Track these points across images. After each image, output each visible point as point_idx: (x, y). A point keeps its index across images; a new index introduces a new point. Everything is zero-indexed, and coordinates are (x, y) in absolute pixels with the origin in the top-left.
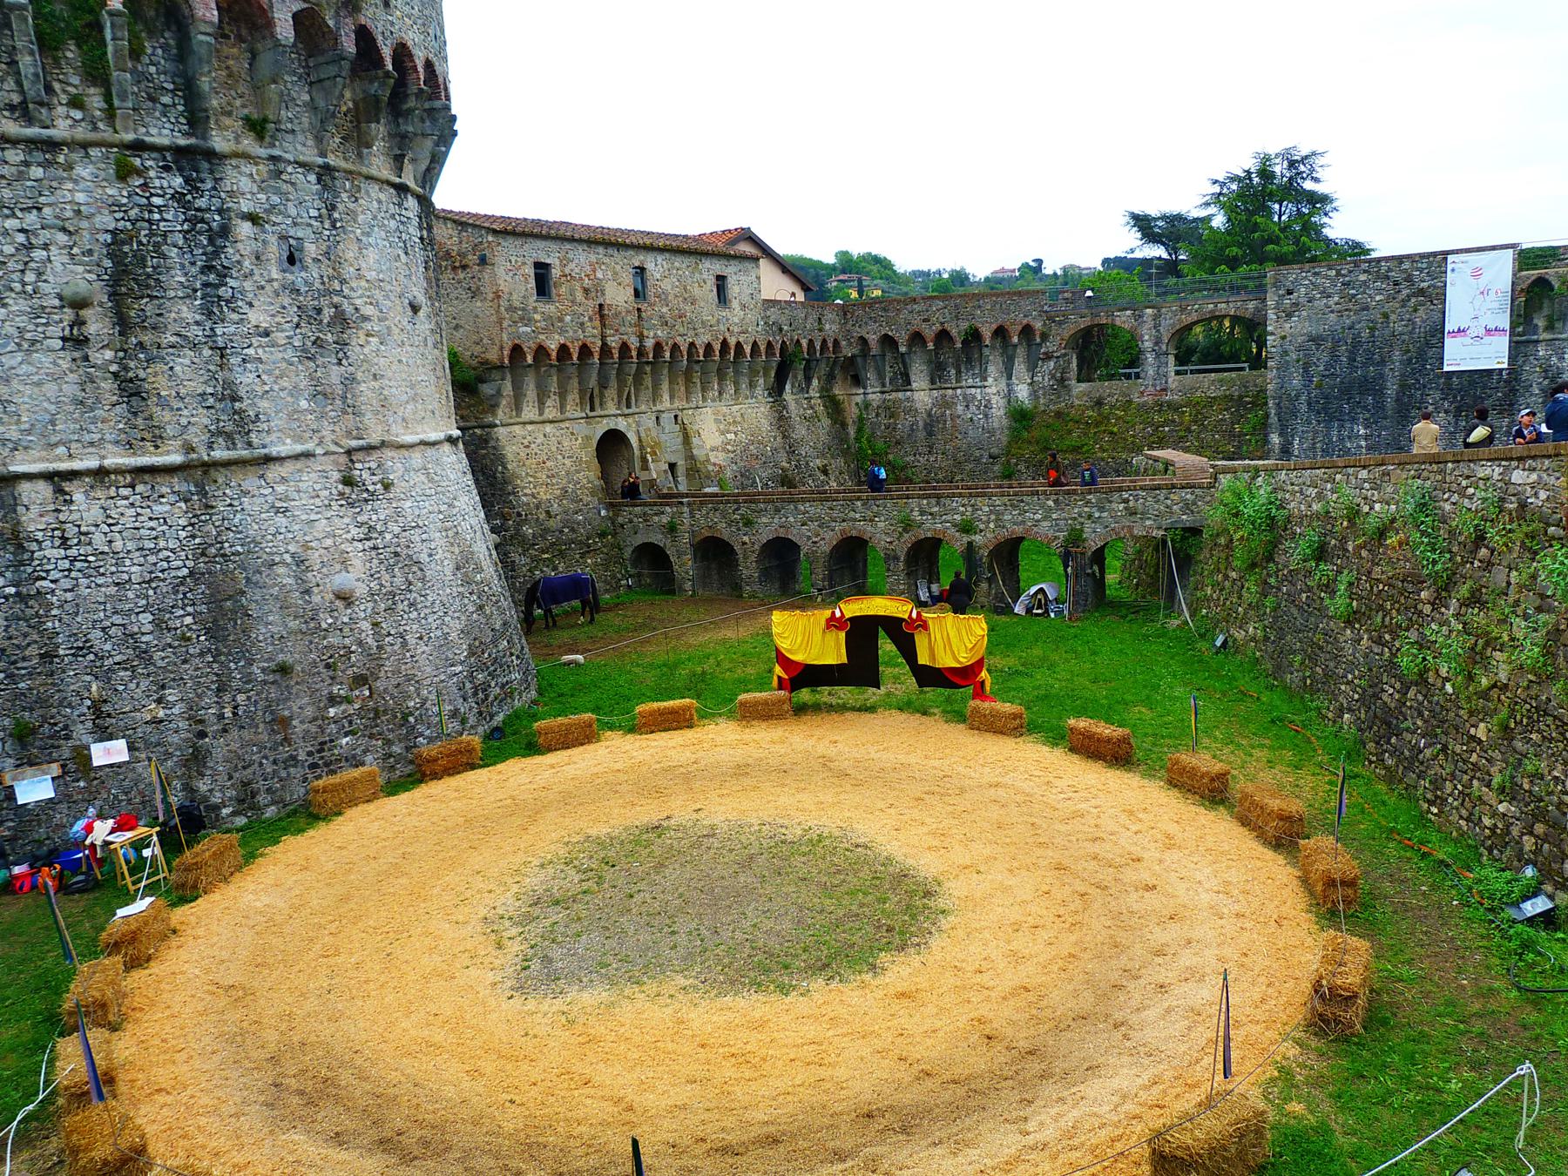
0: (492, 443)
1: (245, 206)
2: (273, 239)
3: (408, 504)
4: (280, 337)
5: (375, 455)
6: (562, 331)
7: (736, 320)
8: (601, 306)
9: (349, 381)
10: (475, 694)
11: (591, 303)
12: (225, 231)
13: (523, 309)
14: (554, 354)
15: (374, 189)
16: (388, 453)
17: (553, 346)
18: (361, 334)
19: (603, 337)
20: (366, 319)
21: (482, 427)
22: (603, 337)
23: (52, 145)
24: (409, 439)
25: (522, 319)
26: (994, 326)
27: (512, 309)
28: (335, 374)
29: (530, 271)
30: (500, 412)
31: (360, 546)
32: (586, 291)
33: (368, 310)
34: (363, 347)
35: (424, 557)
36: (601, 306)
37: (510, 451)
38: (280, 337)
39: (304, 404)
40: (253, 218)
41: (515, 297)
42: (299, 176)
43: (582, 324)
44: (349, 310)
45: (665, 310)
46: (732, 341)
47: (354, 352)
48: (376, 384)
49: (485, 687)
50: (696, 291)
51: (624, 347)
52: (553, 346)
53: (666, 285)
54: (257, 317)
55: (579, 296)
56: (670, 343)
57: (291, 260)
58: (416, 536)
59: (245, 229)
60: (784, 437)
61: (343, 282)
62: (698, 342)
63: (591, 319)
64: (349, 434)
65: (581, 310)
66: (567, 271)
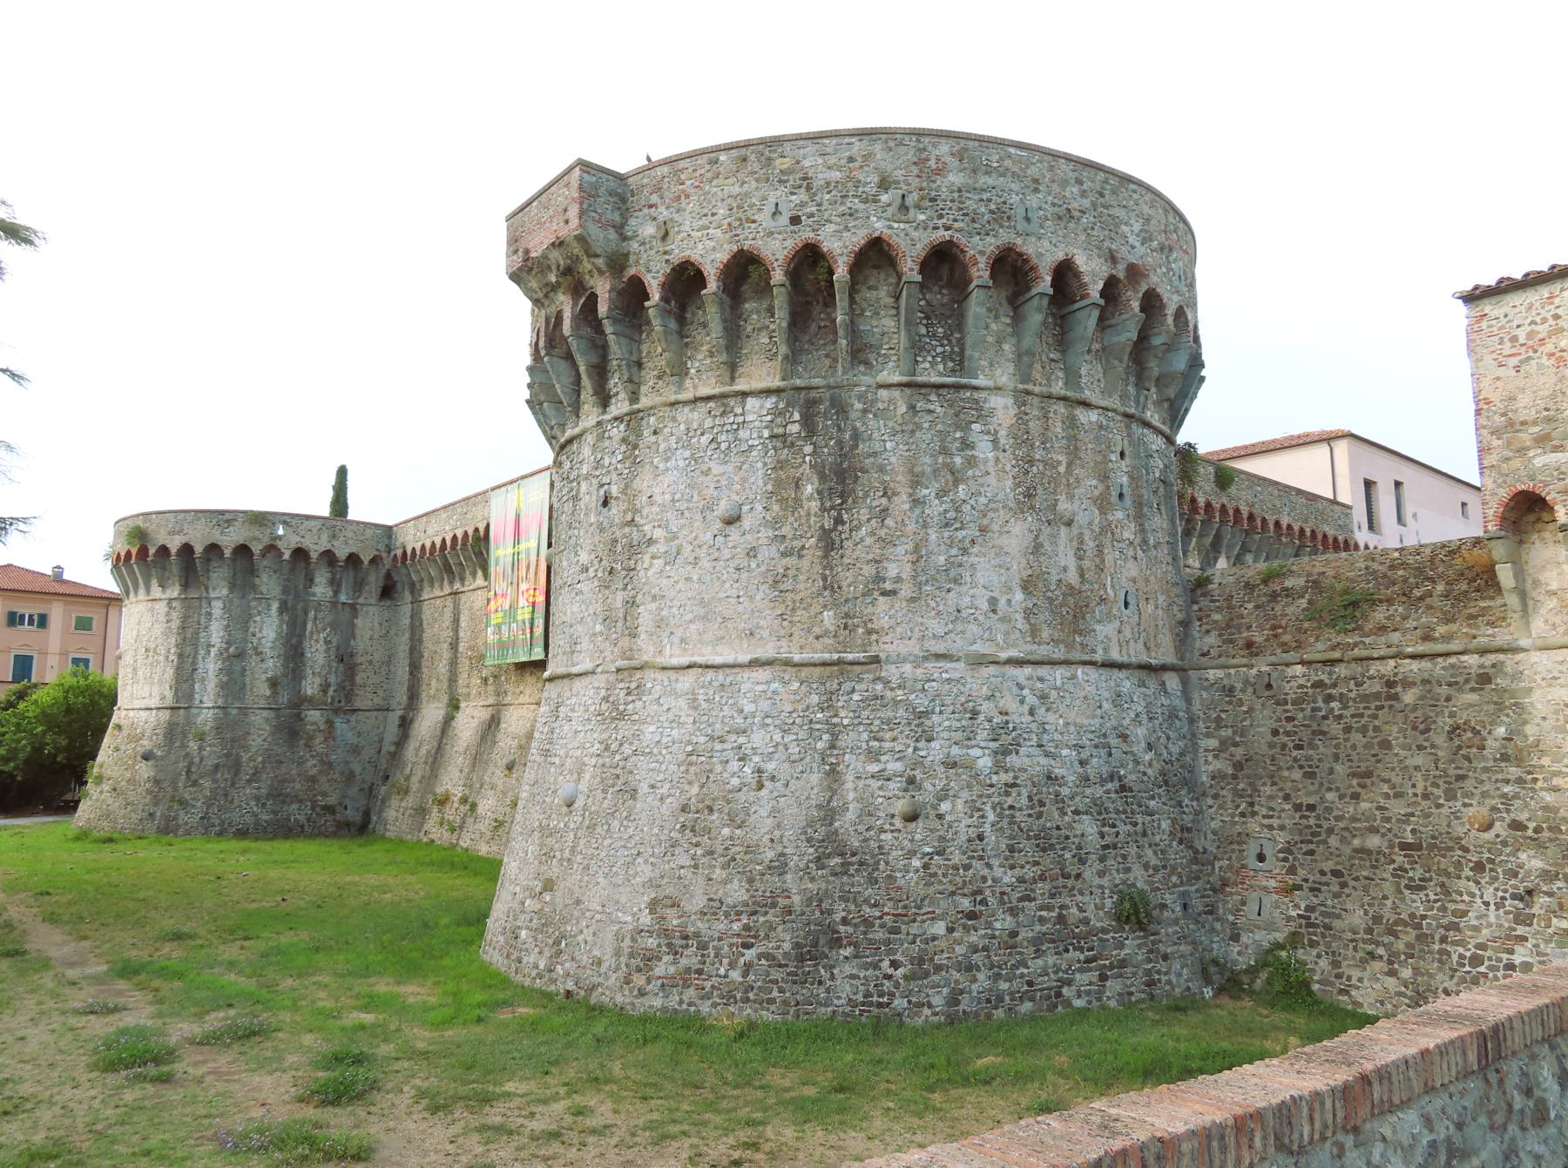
0: (1500, 681)
3: (652, 728)
4: (591, 573)
5: (638, 675)
9: (632, 603)
10: (631, 955)
13: (1549, 420)
15: (684, 414)
16: (650, 675)
20: (651, 542)
21: (1483, 652)
24: (675, 661)
28: (620, 596)
30: (1538, 625)
31: (594, 761)
33: (658, 533)
34: (650, 569)
35: (644, 788)
37: (1541, 701)
39: (598, 628)
41: (1523, 400)
44: (636, 536)
48: (653, 606)
49: (650, 958)
54: (584, 557)
57: (605, 503)
58: (642, 762)
61: (636, 511)
64: (624, 656)
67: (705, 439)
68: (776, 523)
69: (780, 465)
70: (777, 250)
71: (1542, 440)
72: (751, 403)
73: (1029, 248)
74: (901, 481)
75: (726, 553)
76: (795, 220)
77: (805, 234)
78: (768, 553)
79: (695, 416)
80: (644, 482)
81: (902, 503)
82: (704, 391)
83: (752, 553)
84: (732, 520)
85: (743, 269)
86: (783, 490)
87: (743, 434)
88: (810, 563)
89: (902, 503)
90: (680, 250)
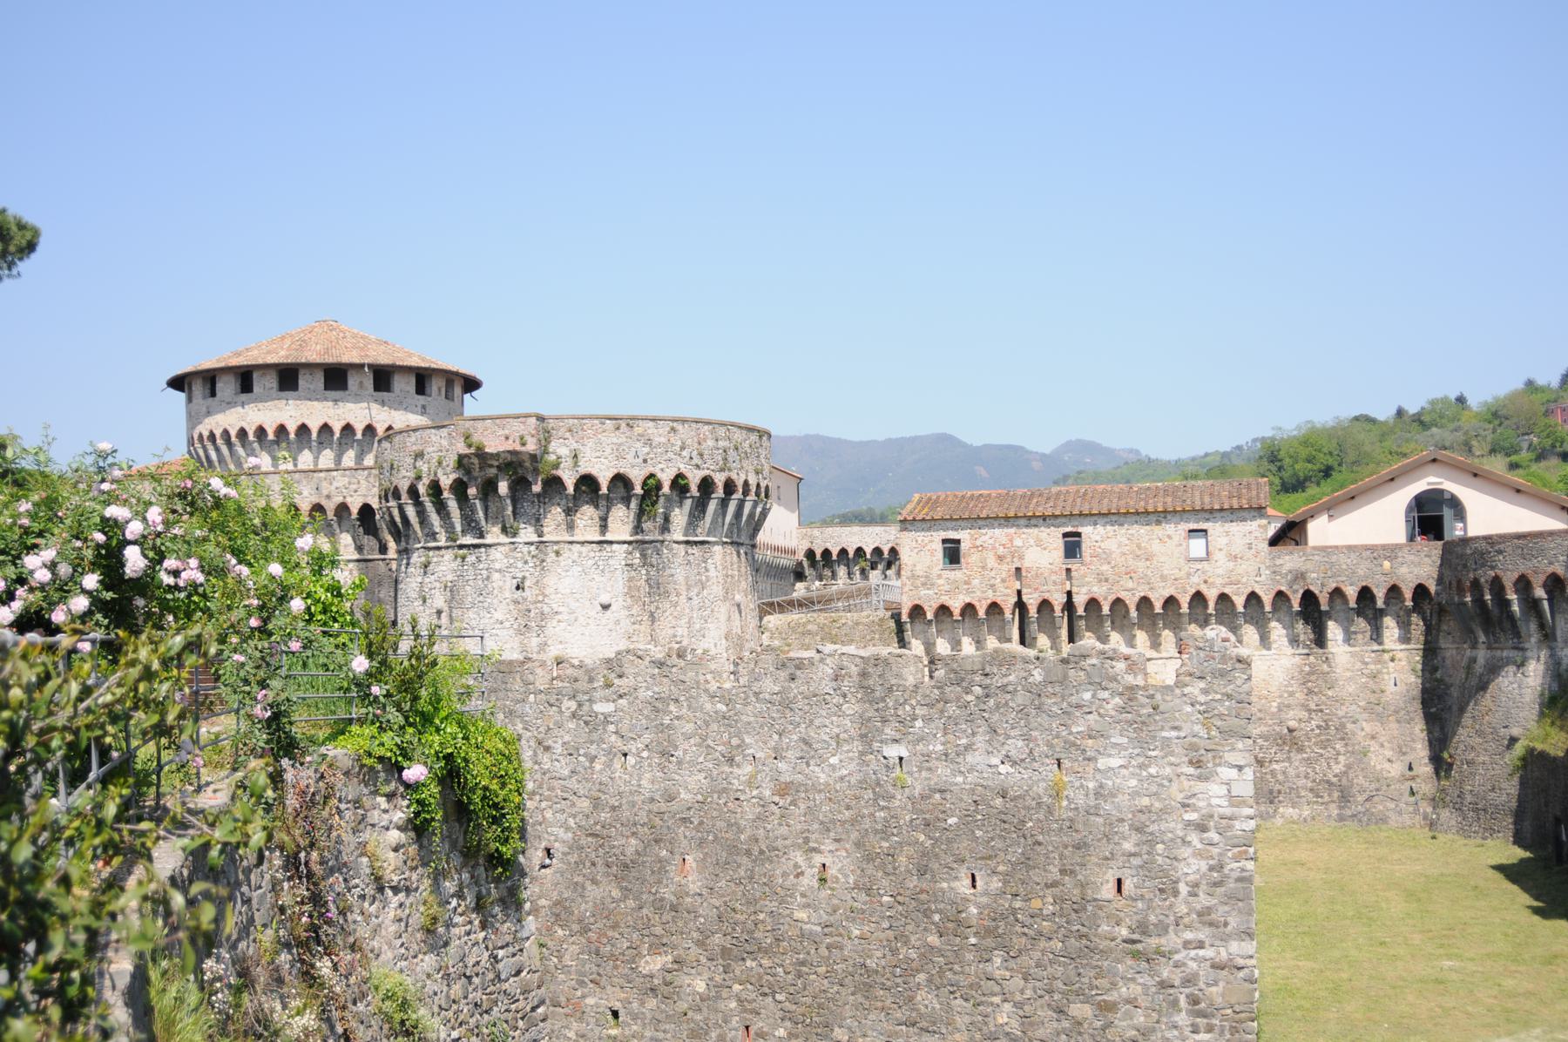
1: (497, 566)
2: (508, 579)
4: (507, 624)
6: (968, 592)
7: (1220, 571)
8: (1018, 570)
11: (1005, 567)
12: (488, 578)
14: (957, 612)
17: (956, 606)
18: (555, 623)
19: (1019, 593)
22: (1019, 593)
23: (439, 548)
25: (924, 584)
26: (1516, 575)
27: (913, 577)
28: (535, 641)
29: (939, 547)
32: (1001, 558)
36: (1018, 570)
38: (507, 624)
40: (499, 571)
42: (525, 549)
43: (992, 586)
44: (546, 609)
45: (1105, 567)
46: (1211, 595)
47: (549, 631)
50: (1156, 547)
51: (1045, 605)
52: (956, 606)
53: (1111, 545)
54: (499, 615)
55: (991, 562)
56: (1111, 598)
57: (518, 588)
59: (496, 576)
60: (1310, 692)
62: (1152, 596)
63: (1003, 581)
65: (993, 574)
66: (978, 543)
67: (591, 562)
68: (629, 608)
69: (630, 580)
70: (637, 476)
71: (924, 584)
72: (615, 546)
73: (734, 476)
74: (682, 588)
75: (604, 622)
76: (645, 461)
77: (650, 469)
78: (626, 624)
79: (585, 549)
80: (551, 581)
81: (683, 599)
82: (590, 538)
83: (617, 622)
84: (606, 607)
85: (620, 480)
86: (631, 592)
87: (611, 562)
88: (645, 628)
89: (683, 599)
90: (584, 469)
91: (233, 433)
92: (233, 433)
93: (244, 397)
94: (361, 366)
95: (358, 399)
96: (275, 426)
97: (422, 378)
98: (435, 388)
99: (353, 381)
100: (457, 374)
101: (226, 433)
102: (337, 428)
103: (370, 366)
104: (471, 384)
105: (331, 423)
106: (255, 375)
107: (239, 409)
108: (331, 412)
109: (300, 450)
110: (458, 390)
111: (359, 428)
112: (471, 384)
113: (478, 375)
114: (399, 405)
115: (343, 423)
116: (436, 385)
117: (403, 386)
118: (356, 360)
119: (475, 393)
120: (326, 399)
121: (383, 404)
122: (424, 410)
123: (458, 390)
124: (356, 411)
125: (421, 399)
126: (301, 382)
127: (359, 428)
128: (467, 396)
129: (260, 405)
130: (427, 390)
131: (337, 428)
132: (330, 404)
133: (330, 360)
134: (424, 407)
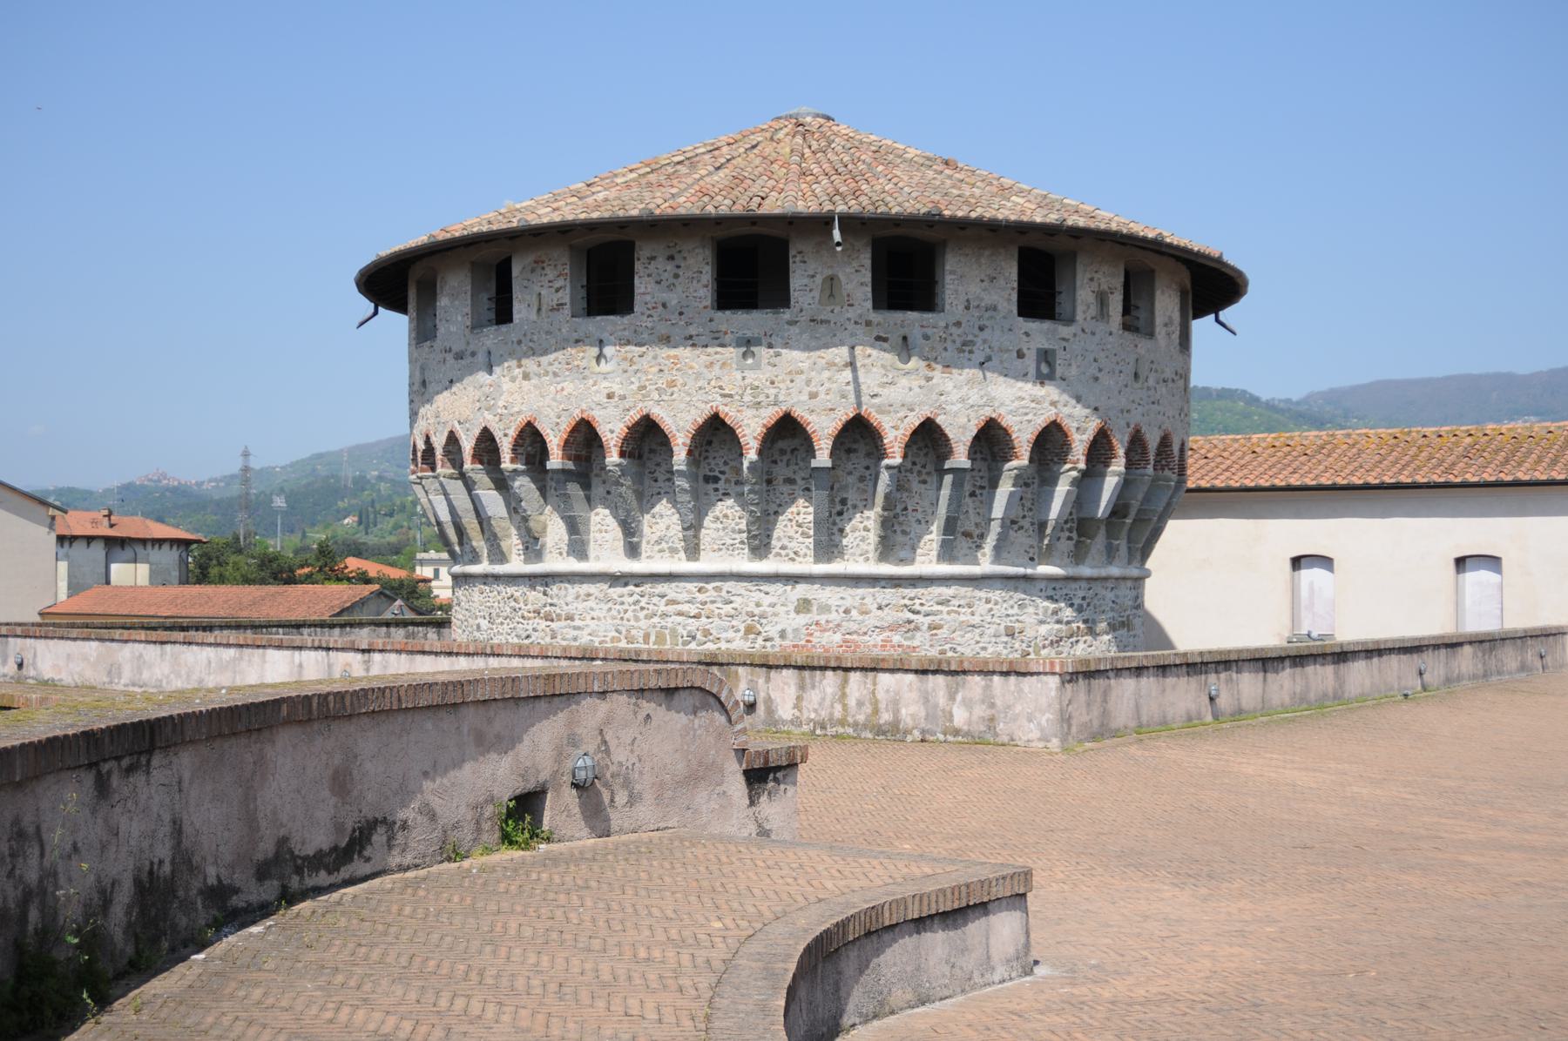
91: (468, 445)
92: (468, 445)
93: (492, 336)
94: (818, 225)
95: (819, 333)
96: (566, 425)
97: (1044, 264)
98: (1084, 296)
99: (803, 279)
100: (1157, 248)
101: (486, 441)
102: (751, 428)
103: (853, 224)
104: (1213, 286)
105: (730, 414)
106: (516, 270)
107: (482, 377)
108: (733, 379)
109: (646, 501)
110: (1166, 304)
111: (824, 428)
112: (1213, 286)
113: (1234, 258)
114: (963, 351)
115: (770, 415)
116: (1090, 287)
117: (974, 289)
118: (806, 205)
119: (1226, 314)
120: (717, 339)
121: (905, 348)
122: (1046, 368)
123: (1166, 304)
124: (814, 376)
125: (1039, 333)
126: (643, 286)
127: (824, 428)
128: (1203, 327)
129: (530, 364)
130: (1062, 301)
131: (751, 428)
132: (731, 353)
133: (723, 206)
134: (1046, 356)
